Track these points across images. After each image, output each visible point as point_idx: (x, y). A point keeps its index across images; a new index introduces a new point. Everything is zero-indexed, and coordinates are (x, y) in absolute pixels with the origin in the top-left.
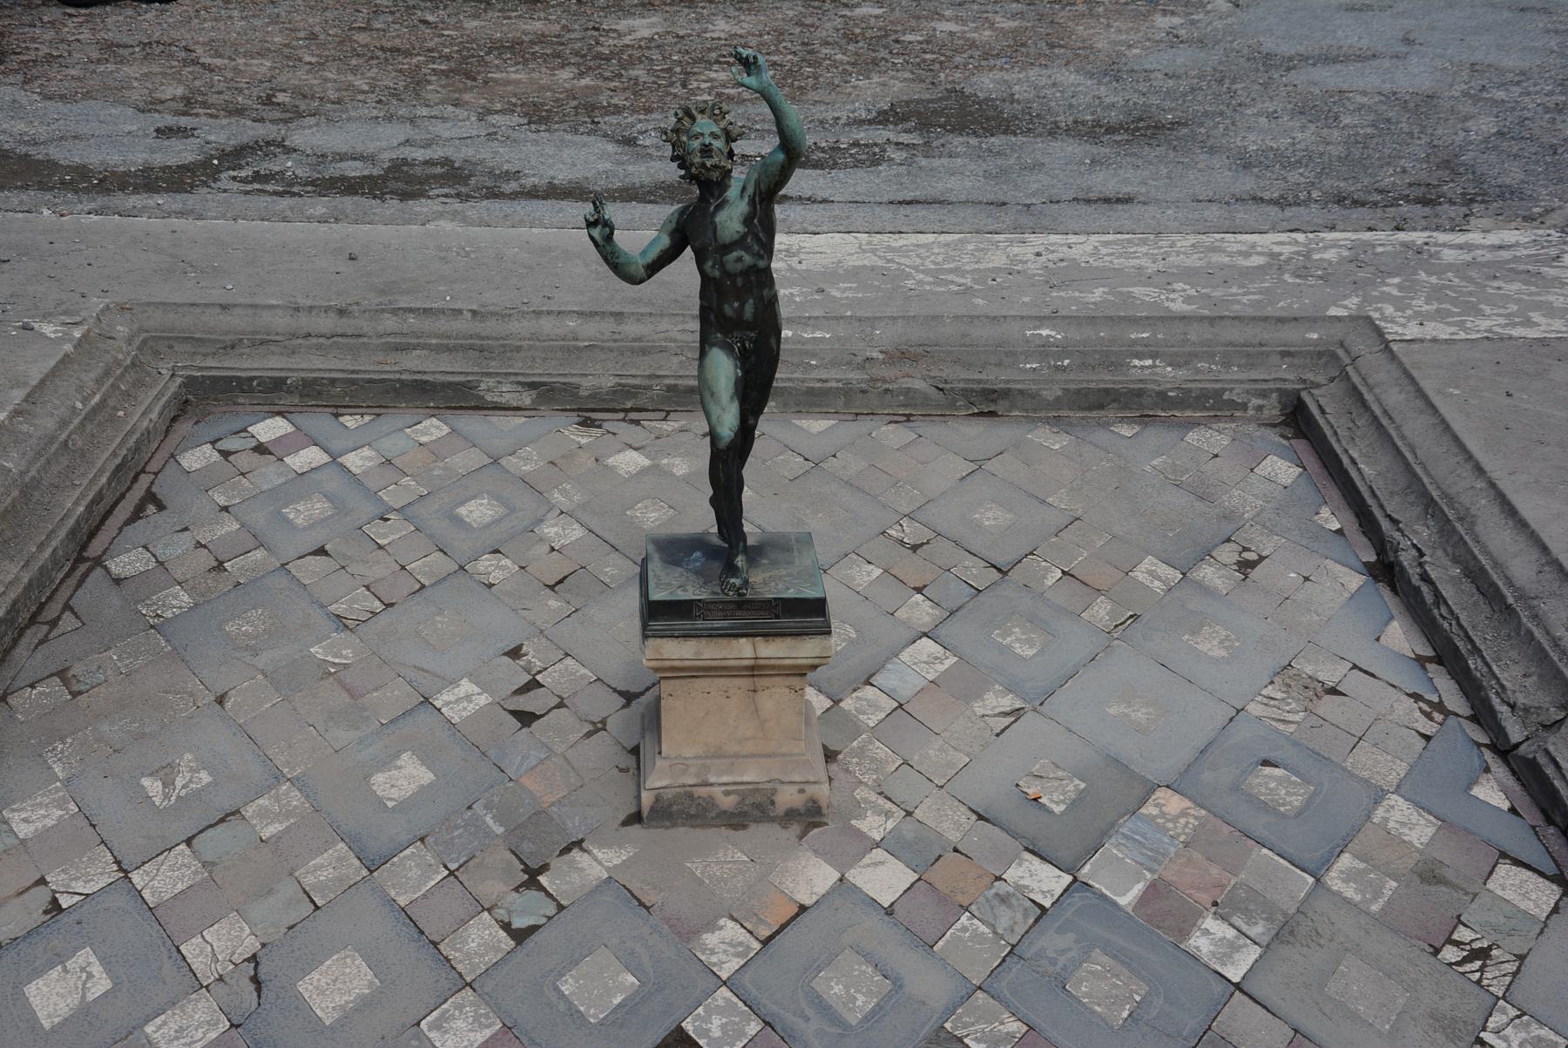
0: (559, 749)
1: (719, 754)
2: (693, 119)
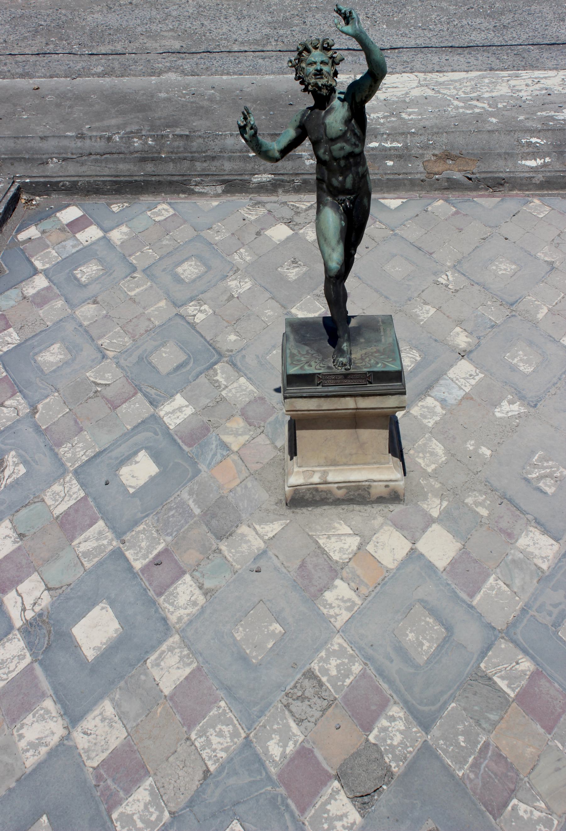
0: (235, 448)
1: (334, 463)
2: (309, 51)
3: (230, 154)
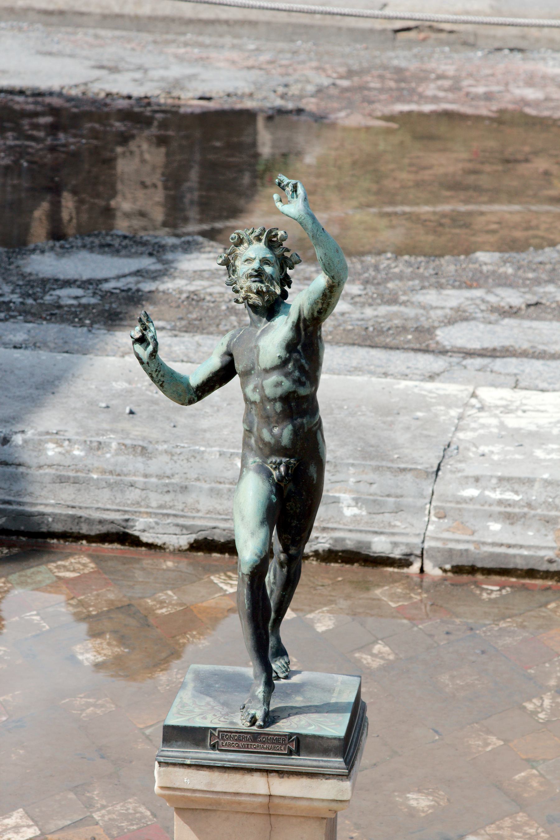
3: (213, 485)
